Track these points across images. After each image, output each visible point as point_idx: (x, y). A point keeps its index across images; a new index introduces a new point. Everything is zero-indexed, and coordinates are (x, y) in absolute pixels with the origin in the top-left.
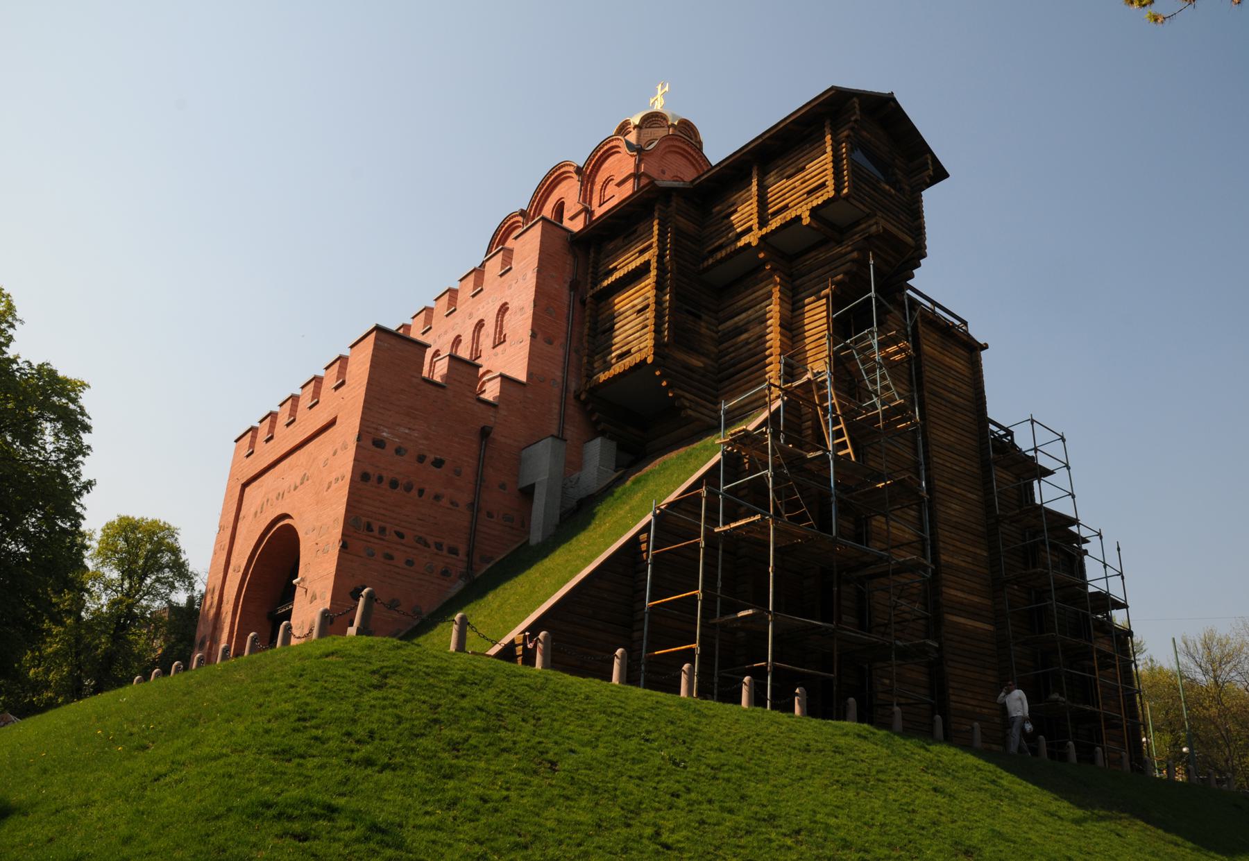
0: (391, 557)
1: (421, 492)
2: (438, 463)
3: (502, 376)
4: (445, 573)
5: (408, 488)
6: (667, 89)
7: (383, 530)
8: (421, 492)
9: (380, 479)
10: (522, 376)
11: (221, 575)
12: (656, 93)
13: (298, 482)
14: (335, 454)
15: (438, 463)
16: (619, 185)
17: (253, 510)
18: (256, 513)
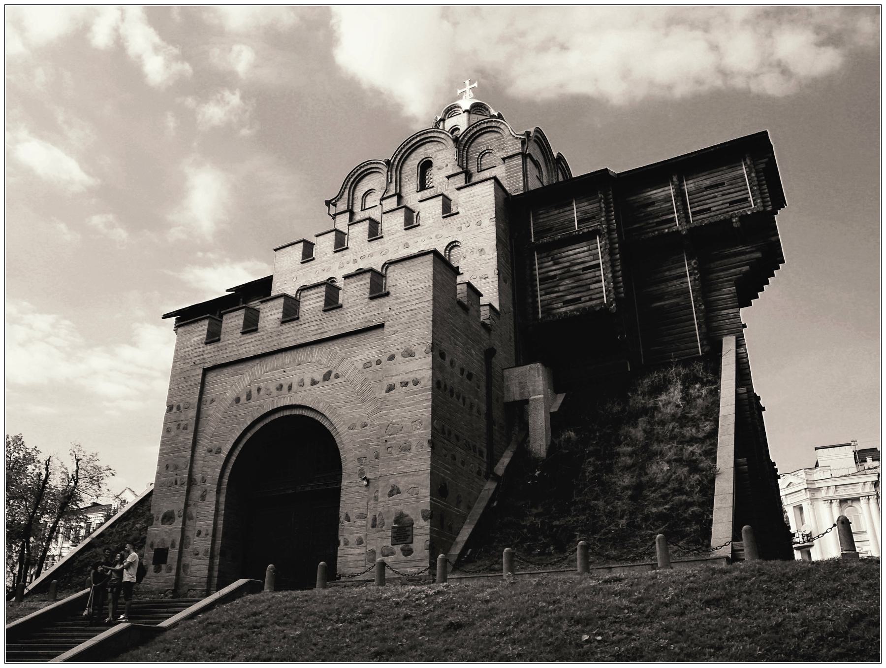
0: (454, 458)
1: (464, 399)
2: (470, 376)
3: (490, 305)
4: (479, 473)
5: (458, 398)
6: (476, 85)
7: (450, 433)
8: (464, 399)
9: (445, 386)
10: (497, 306)
11: (188, 454)
12: (464, 86)
13: (318, 377)
14: (392, 358)
15: (470, 376)
16: (504, 159)
17: (230, 395)
18: (238, 400)
